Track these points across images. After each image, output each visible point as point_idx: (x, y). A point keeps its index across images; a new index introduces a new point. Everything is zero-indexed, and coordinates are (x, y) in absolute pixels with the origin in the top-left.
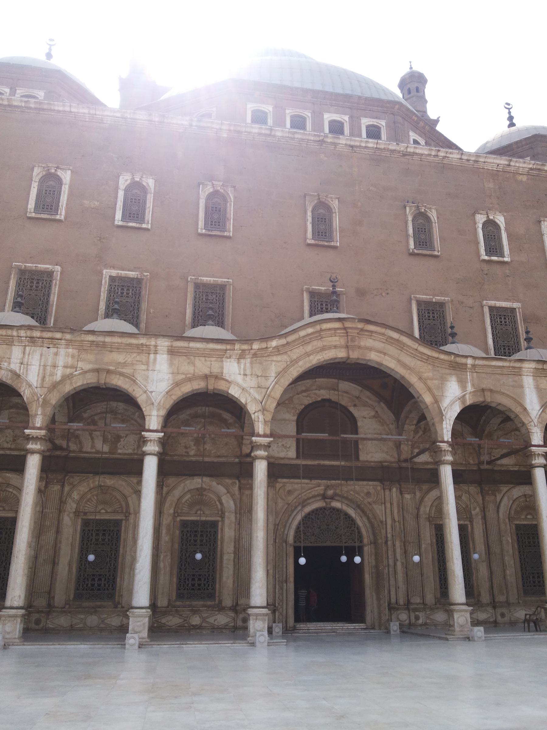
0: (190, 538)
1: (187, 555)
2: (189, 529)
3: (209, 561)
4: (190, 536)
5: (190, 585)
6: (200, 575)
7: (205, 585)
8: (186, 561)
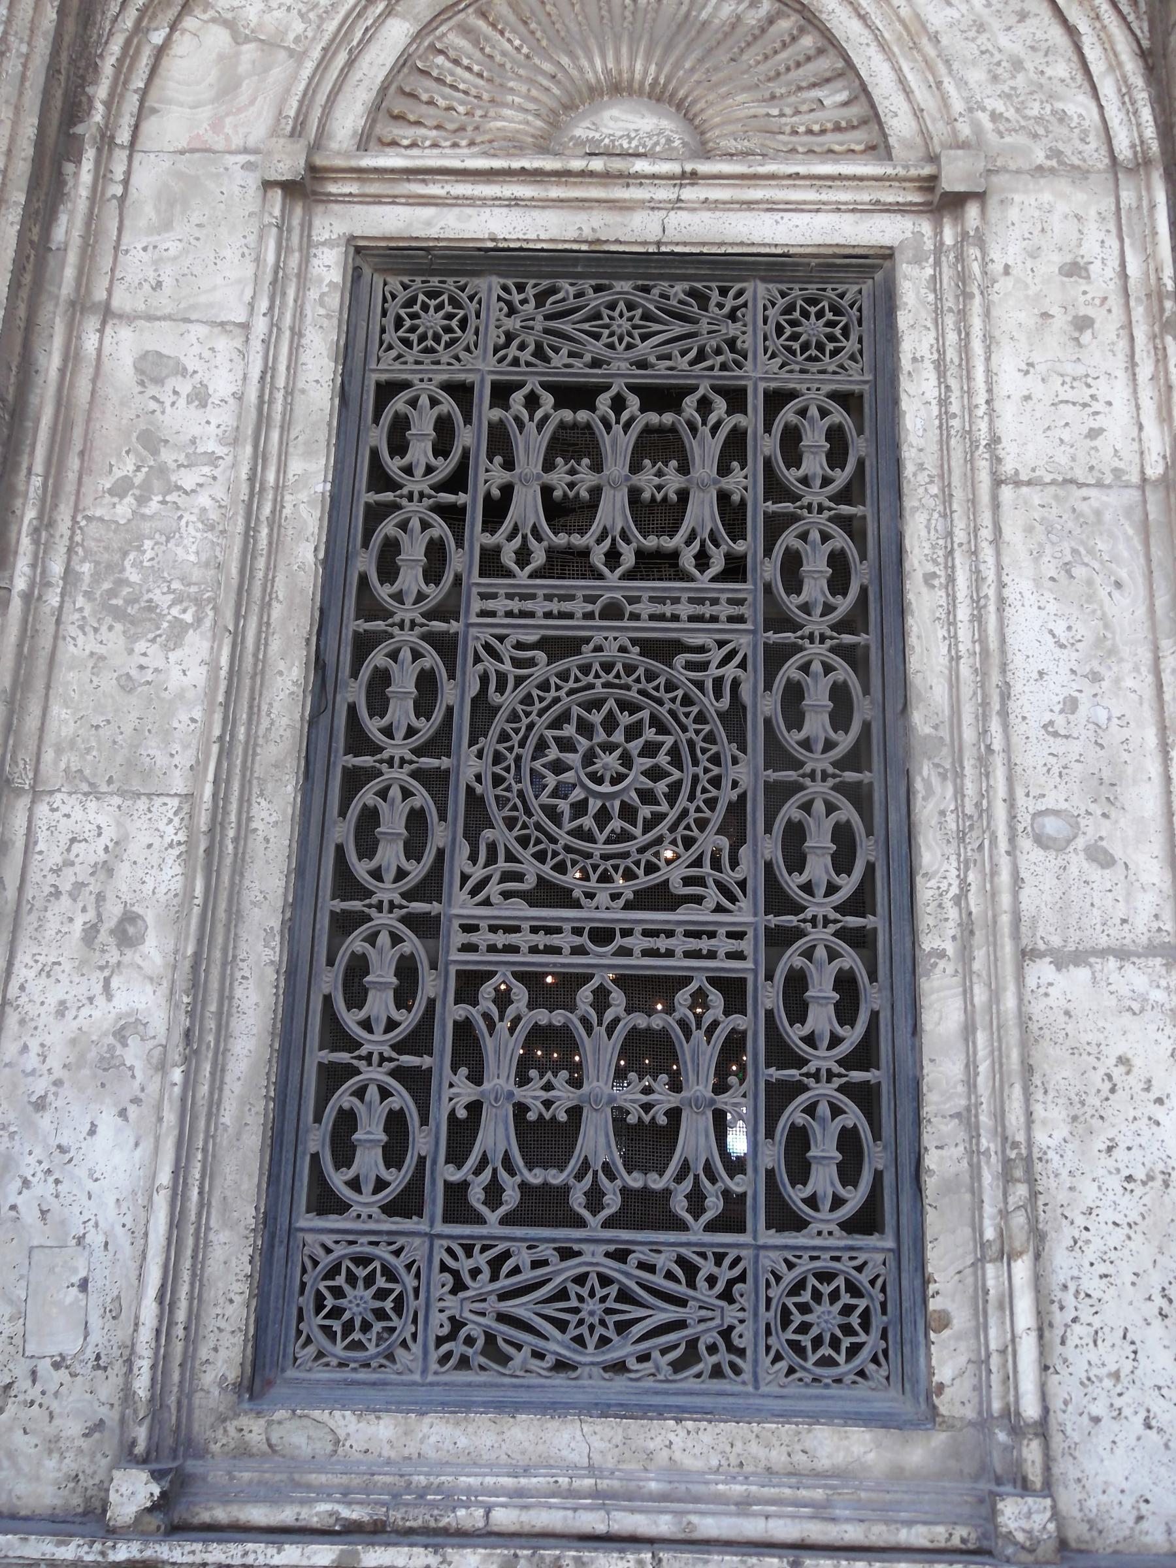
0: (488, 476)
2: (482, 369)
3: (777, 794)
4: (500, 443)
5: (496, 1136)
8: (436, 782)
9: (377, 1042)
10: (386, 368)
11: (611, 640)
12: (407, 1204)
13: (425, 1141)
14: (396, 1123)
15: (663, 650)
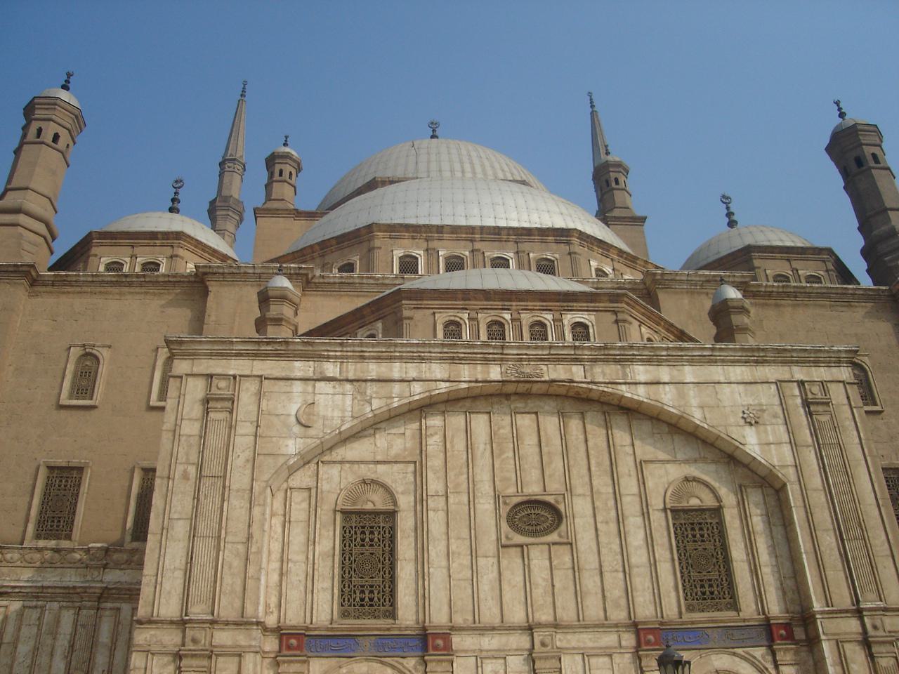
1: (352, 559)
2: (354, 525)
6: (371, 586)
7: (379, 600)
9: (346, 592)
10: (344, 525)
11: (367, 553)
12: (350, 606)
13: (352, 600)
14: (349, 599)
15: (372, 554)
